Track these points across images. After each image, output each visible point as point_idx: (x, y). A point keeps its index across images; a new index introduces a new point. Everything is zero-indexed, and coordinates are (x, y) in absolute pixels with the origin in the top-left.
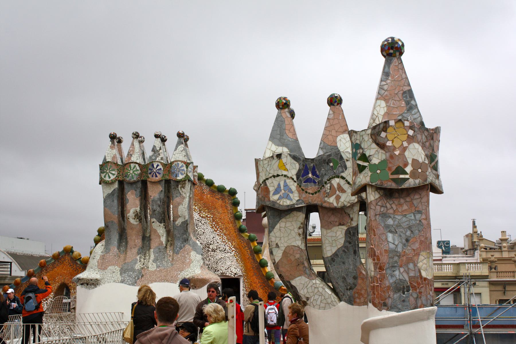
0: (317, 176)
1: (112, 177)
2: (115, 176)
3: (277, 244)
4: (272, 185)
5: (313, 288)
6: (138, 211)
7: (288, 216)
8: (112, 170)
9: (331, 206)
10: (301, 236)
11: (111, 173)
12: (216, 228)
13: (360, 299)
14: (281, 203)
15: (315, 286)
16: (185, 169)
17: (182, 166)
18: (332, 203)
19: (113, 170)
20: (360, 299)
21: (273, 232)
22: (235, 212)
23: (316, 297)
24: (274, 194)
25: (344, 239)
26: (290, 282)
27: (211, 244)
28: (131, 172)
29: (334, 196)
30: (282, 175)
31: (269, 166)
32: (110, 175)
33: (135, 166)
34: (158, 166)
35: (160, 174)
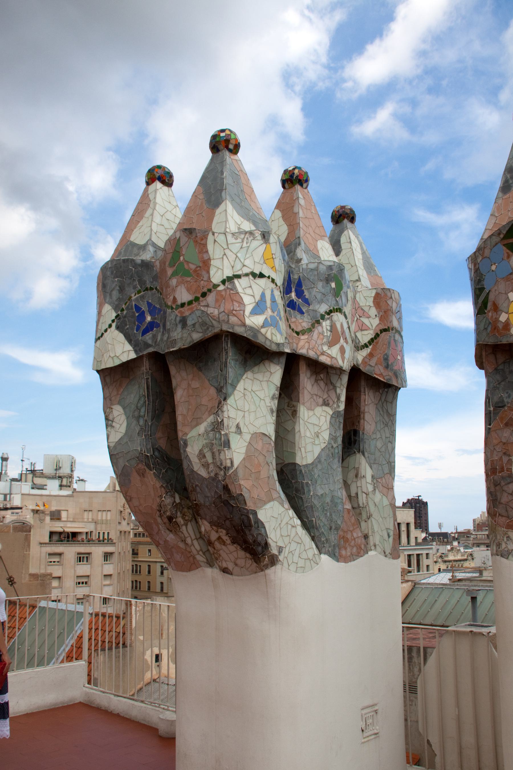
0: (307, 302)
3: (238, 427)
4: (249, 291)
5: (290, 527)
7: (256, 369)
9: (333, 363)
10: (275, 414)
13: (346, 549)
14: (269, 335)
15: (291, 522)
18: (336, 359)
20: (346, 549)
21: (232, 397)
23: (294, 546)
24: (254, 312)
25: (328, 432)
26: (255, 513)
29: (337, 347)
30: (269, 277)
31: (244, 250)
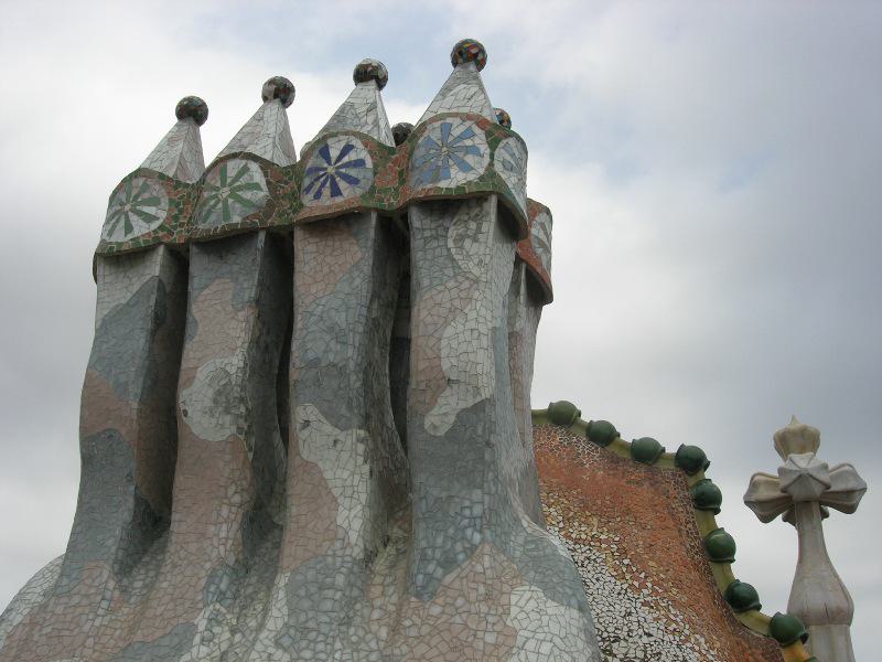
1: (141, 229)
2: (155, 225)
6: (233, 370)
8: (149, 202)
11: (140, 214)
12: (638, 579)
16: (484, 149)
17: (469, 134)
19: (155, 202)
22: (703, 532)
27: (617, 639)
28: (225, 192)
32: (134, 218)
33: (245, 170)
34: (348, 149)
35: (353, 181)
